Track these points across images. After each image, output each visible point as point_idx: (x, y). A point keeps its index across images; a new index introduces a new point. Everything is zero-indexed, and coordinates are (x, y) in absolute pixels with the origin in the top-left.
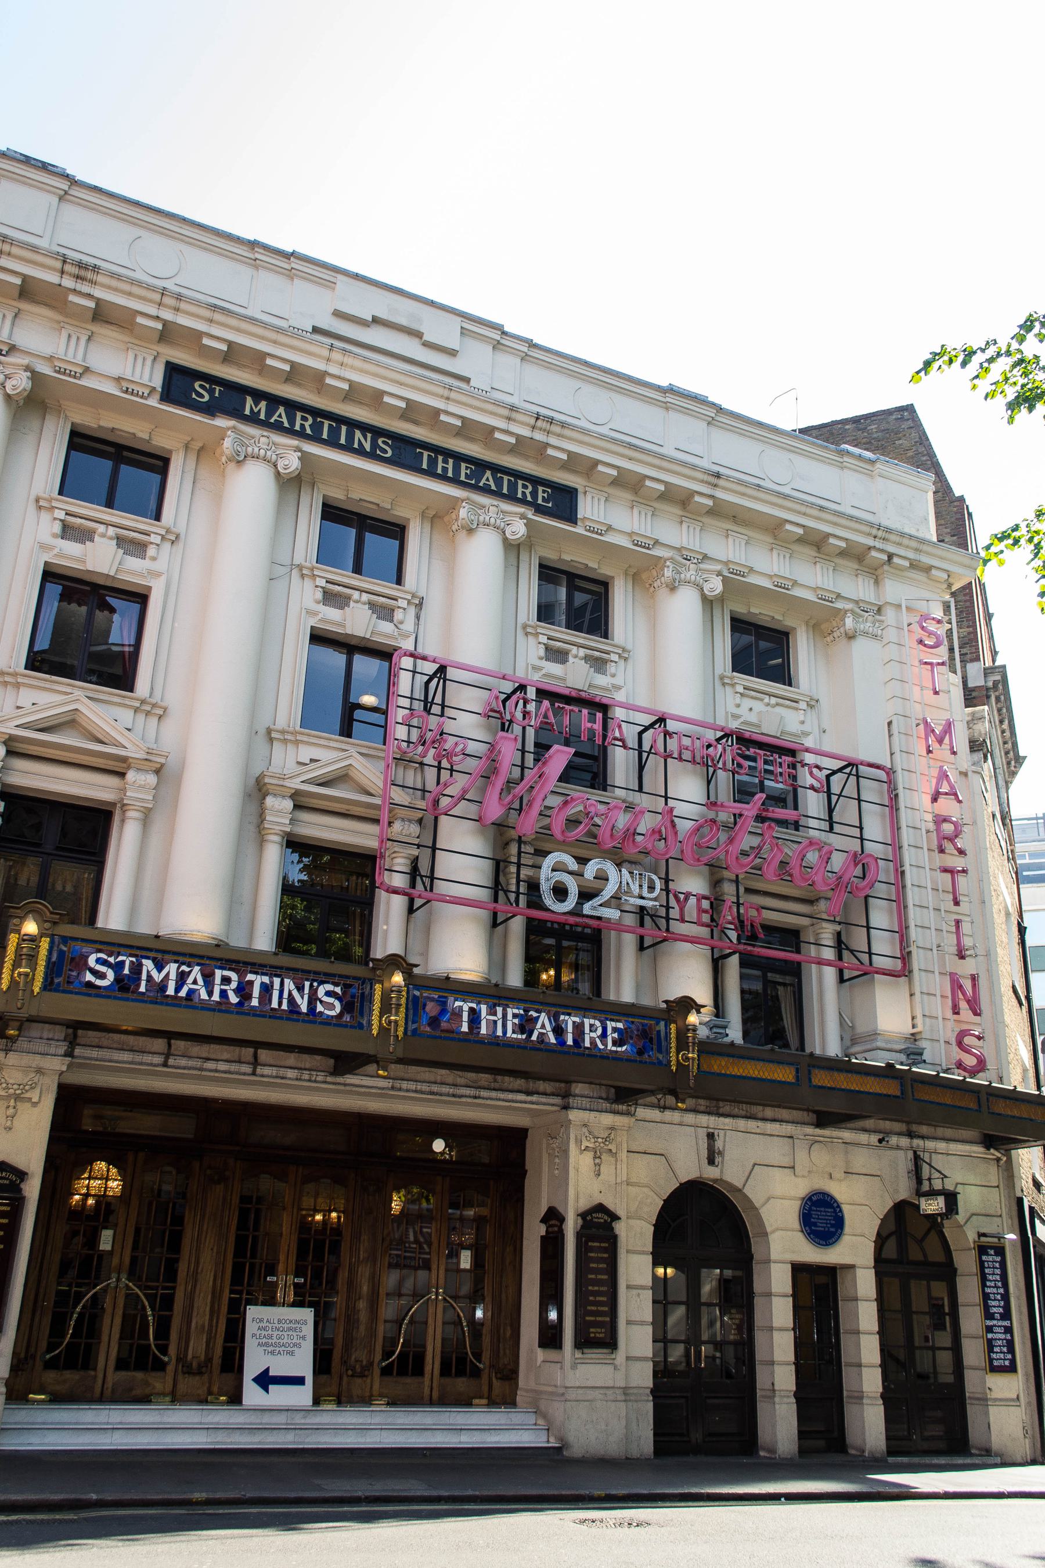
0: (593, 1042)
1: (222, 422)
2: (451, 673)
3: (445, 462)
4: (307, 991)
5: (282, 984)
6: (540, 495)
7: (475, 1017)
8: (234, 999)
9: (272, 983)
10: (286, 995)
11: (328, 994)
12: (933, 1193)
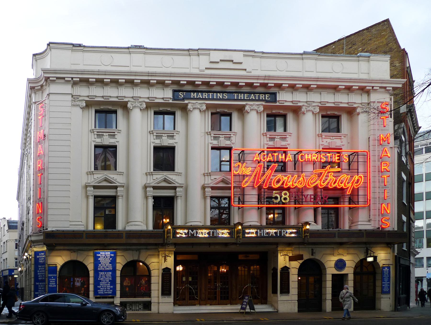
1: (186, 102)
2: (245, 152)
3: (241, 95)
6: (267, 97)
12: (371, 256)
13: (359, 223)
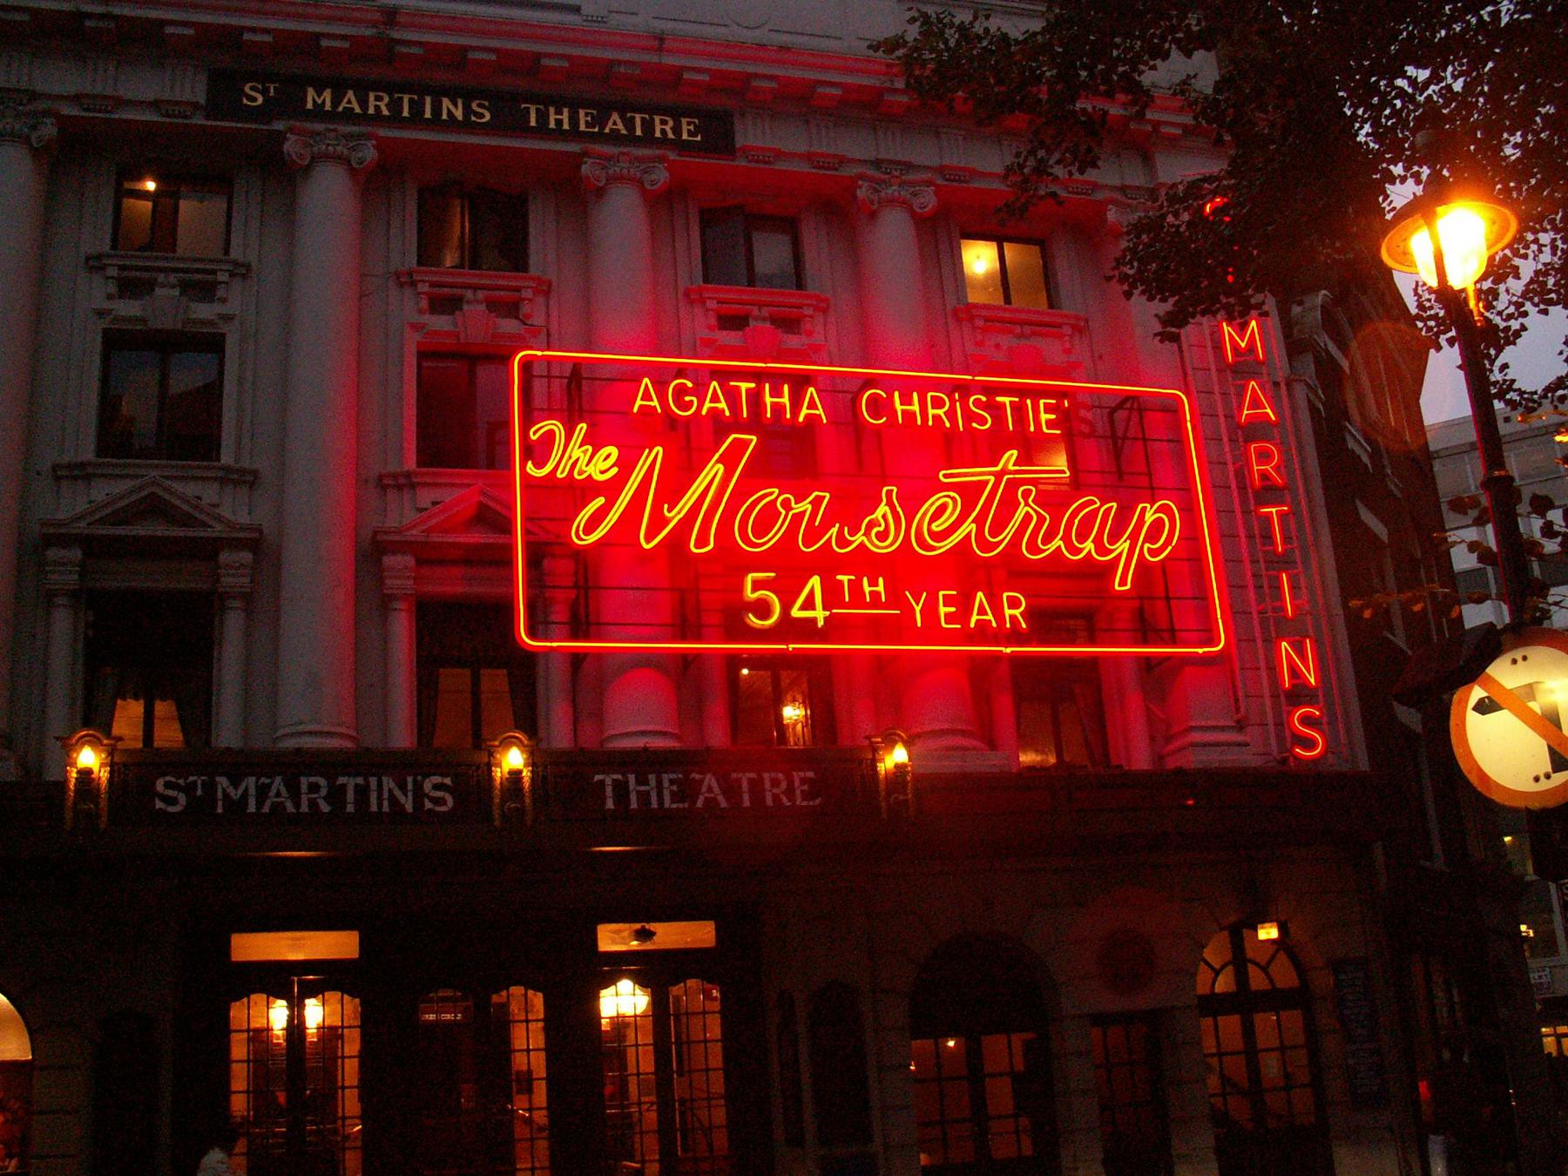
0: (776, 798)
1: (279, 126)
4: (410, 787)
5: (380, 785)
6: (685, 128)
7: (621, 789)
8: (325, 808)
9: (368, 784)
10: (386, 795)
11: (436, 787)
13: (1197, 737)
